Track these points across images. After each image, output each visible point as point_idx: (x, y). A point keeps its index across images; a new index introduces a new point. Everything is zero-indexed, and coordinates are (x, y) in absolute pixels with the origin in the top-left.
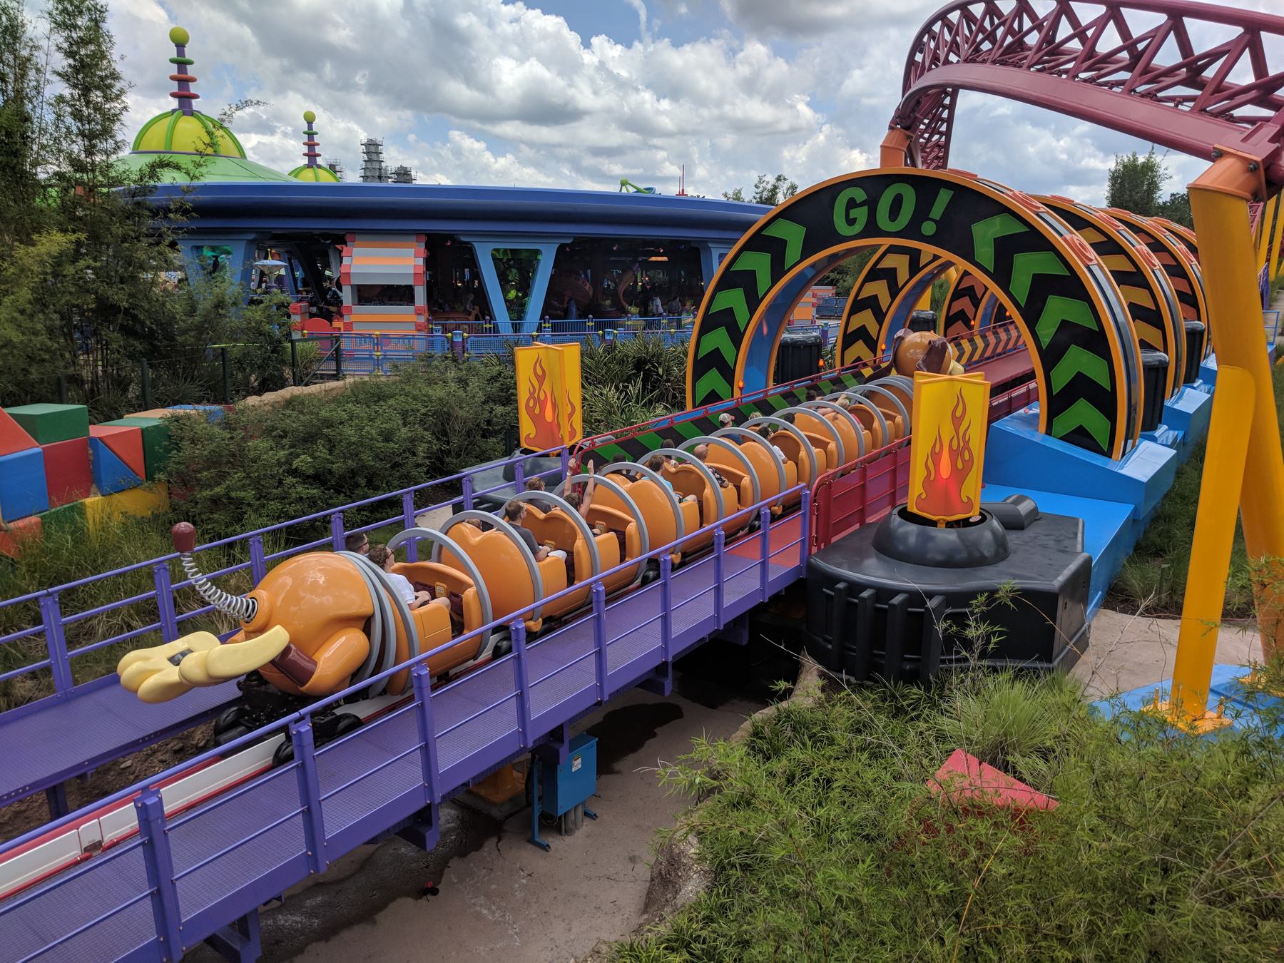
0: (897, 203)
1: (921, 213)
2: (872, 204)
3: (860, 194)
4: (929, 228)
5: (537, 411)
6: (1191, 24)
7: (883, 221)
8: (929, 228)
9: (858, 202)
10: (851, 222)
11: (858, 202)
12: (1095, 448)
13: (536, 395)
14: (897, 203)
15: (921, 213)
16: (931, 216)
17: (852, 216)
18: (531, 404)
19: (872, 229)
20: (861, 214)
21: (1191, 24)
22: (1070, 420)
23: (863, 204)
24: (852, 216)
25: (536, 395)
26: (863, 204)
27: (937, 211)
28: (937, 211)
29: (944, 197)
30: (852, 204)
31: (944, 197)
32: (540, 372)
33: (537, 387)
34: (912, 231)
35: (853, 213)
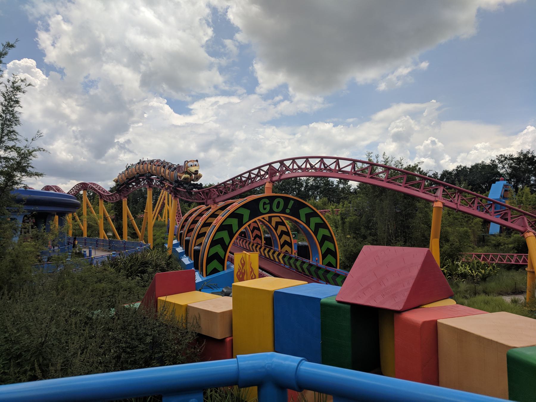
0: (279, 203)
1: (286, 207)
2: (271, 204)
3: (267, 201)
4: (288, 211)
5: (241, 276)
6: (325, 160)
7: (275, 209)
8: (288, 211)
10: (265, 209)
12: (333, 267)
13: (241, 271)
14: (279, 203)
15: (286, 207)
17: (265, 207)
18: (239, 273)
19: (271, 211)
20: (268, 207)
21: (325, 160)
22: (327, 260)
23: (268, 204)
24: (265, 207)
25: (241, 271)
27: (290, 206)
28: (290, 206)
29: (292, 203)
30: (265, 204)
31: (292, 203)
32: (243, 262)
33: (241, 267)
34: (283, 212)
35: (265, 206)
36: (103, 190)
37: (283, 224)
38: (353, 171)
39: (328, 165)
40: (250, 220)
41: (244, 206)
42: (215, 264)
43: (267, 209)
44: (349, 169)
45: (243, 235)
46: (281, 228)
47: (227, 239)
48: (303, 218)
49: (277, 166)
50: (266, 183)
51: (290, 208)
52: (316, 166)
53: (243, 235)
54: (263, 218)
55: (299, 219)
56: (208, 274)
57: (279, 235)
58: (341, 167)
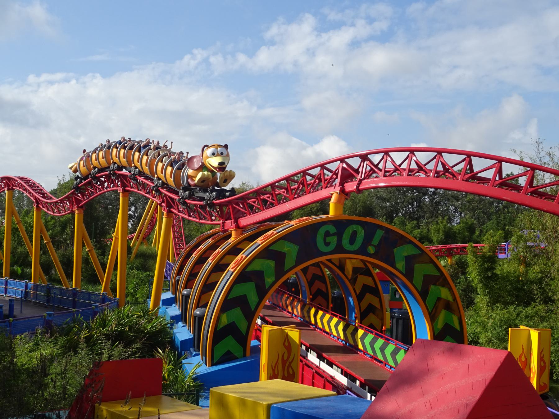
0: (354, 235)
2: (339, 235)
3: (332, 229)
4: (371, 250)
9: (331, 233)
10: (327, 244)
11: (331, 233)
14: (354, 235)
16: (373, 243)
19: (339, 249)
20: (333, 240)
23: (334, 234)
26: (334, 234)
27: (376, 241)
28: (376, 241)
29: (379, 234)
30: (327, 234)
31: (379, 234)
34: (362, 251)
35: (329, 239)
36: (42, 192)
37: (368, 273)
38: (497, 178)
39: (451, 166)
40: (298, 263)
41: (289, 237)
42: (230, 344)
43: (331, 244)
44: (489, 174)
45: (293, 289)
46: (363, 280)
47: (253, 298)
48: (401, 265)
49: (355, 163)
50: (332, 194)
51: (376, 244)
52: (428, 167)
53: (293, 289)
54: (330, 260)
55: (393, 265)
56: (215, 361)
57: (358, 292)
58: (475, 170)
